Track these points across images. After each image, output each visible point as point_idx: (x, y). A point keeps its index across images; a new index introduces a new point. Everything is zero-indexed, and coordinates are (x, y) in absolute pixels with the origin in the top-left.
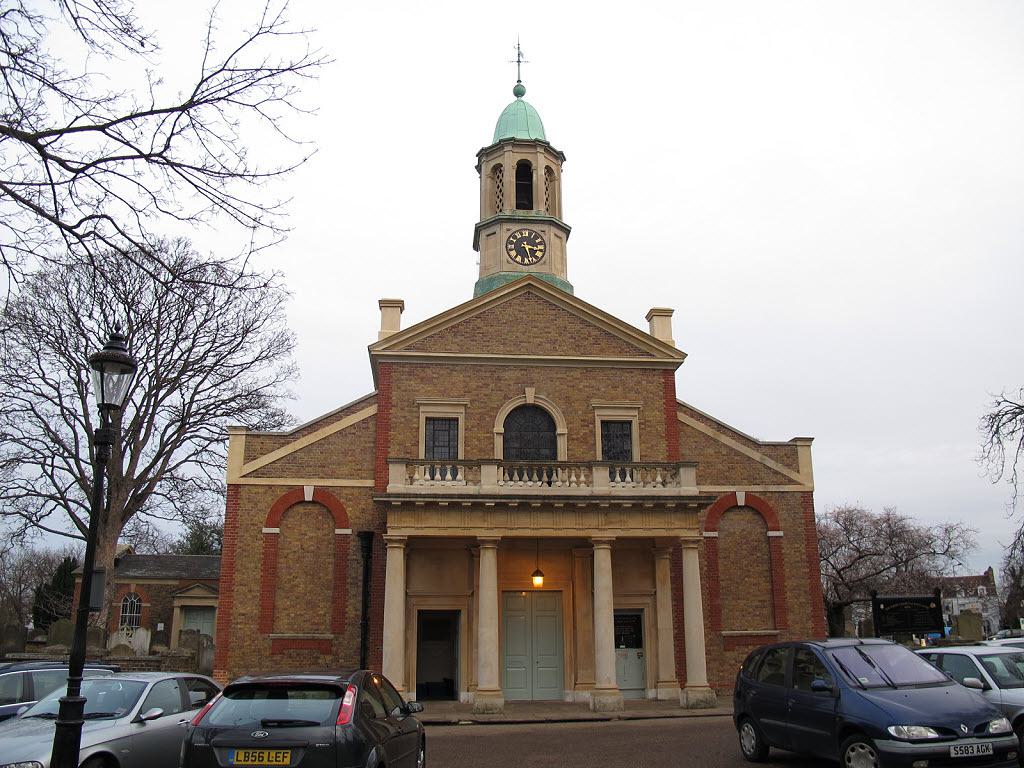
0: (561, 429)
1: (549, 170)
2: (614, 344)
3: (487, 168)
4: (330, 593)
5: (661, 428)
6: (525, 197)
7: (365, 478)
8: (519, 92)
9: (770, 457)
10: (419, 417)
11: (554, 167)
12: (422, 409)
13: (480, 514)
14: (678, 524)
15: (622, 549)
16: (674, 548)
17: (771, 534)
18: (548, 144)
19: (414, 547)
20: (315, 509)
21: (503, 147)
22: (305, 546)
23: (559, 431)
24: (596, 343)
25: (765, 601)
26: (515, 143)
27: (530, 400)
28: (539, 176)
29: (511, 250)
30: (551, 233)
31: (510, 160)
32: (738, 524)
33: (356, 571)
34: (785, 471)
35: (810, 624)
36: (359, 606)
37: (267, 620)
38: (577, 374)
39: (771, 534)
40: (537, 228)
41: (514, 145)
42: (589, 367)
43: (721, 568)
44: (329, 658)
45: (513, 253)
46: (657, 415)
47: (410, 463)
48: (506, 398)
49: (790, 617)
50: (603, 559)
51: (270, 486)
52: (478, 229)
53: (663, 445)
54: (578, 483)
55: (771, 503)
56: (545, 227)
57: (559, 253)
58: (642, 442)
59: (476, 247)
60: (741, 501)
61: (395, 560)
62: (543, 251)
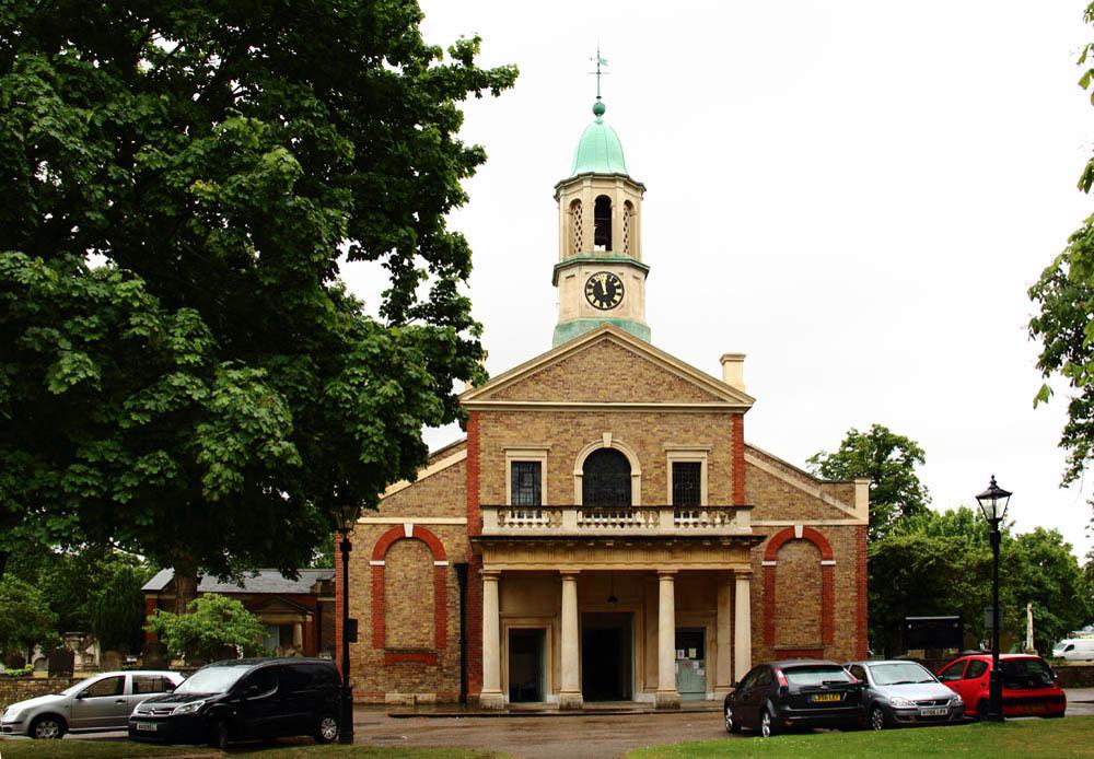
0: (636, 470)
1: (628, 204)
2: (688, 390)
3: (566, 201)
4: (432, 615)
5: (729, 469)
6: (604, 235)
7: (459, 516)
8: (599, 111)
9: (830, 494)
10: (505, 461)
11: (633, 201)
12: (508, 453)
13: (561, 551)
14: (733, 559)
15: (680, 579)
16: (727, 579)
17: (824, 563)
18: (628, 177)
19: (504, 579)
20: (415, 544)
21: (581, 182)
22: (408, 576)
23: (633, 473)
24: (670, 389)
25: (813, 621)
26: (595, 177)
27: (607, 444)
28: (618, 211)
29: (590, 294)
30: (626, 276)
31: (588, 195)
32: (794, 554)
33: (454, 595)
34: (842, 507)
35: (854, 640)
36: (459, 625)
37: (379, 637)
38: (651, 419)
39: (824, 563)
40: (615, 270)
41: (593, 180)
42: (663, 412)
43: (777, 592)
44: (434, 668)
45: (592, 298)
46: (724, 457)
47: (500, 508)
48: (585, 442)
49: (837, 633)
50: (666, 589)
51: (374, 525)
52: (557, 271)
53: (729, 484)
54: (647, 524)
55: (826, 536)
56: (624, 270)
57: (637, 295)
58: (709, 481)
59: (555, 282)
60: (799, 534)
61: (490, 591)
62: (621, 295)
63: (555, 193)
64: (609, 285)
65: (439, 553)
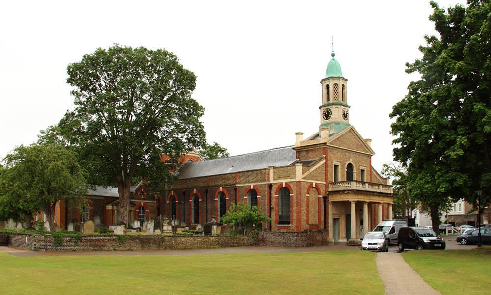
8: (333, 55)
18: (343, 78)
26: (333, 78)
63: (320, 81)
64: (329, 113)
65: (319, 193)
